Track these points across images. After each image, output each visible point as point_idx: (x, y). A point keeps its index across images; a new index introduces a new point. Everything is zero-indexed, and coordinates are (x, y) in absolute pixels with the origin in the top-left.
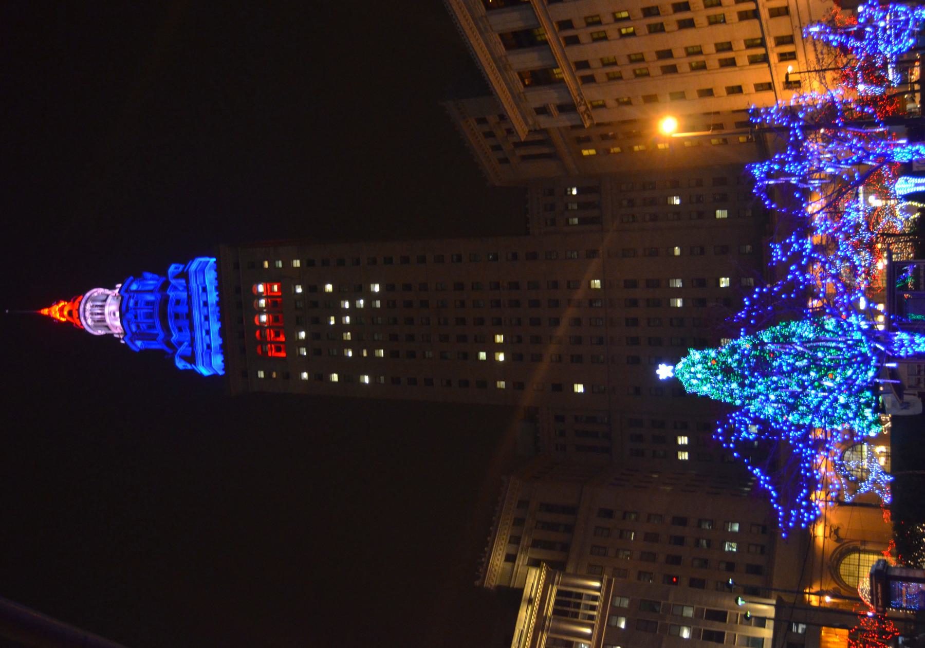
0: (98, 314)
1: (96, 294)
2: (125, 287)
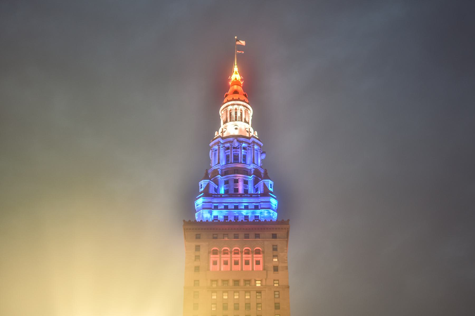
0: (236, 117)
1: (249, 112)
2: (256, 141)
